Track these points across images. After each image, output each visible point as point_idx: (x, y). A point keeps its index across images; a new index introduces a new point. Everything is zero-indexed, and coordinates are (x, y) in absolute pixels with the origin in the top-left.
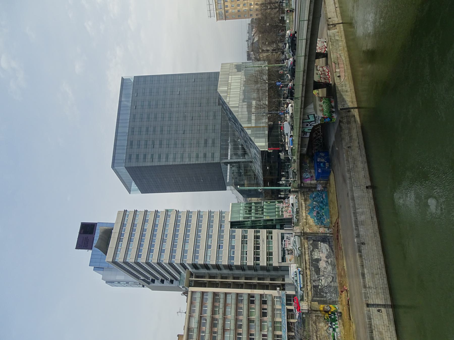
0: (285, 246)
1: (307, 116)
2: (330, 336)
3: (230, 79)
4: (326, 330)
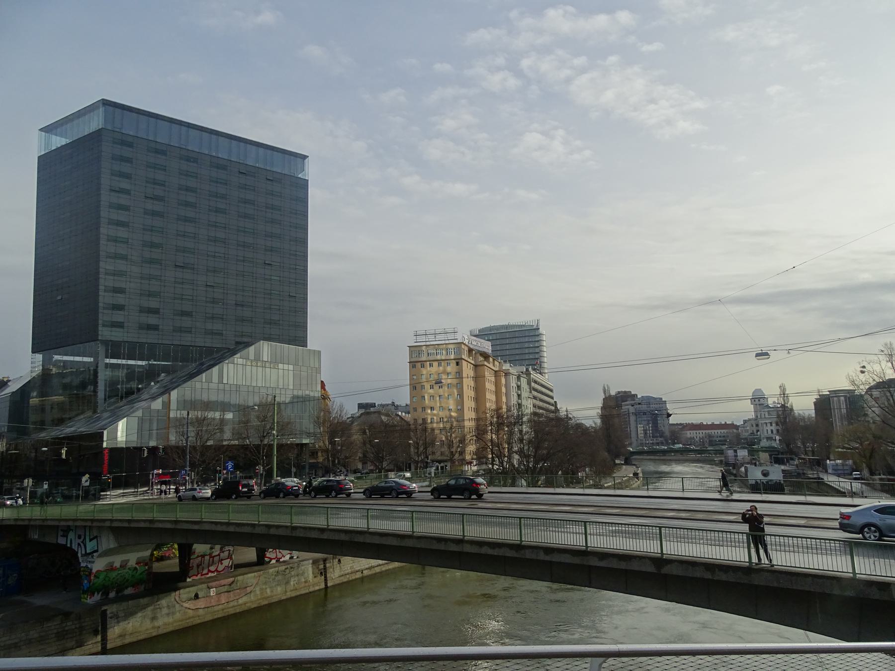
1: (95, 535)
3: (286, 367)
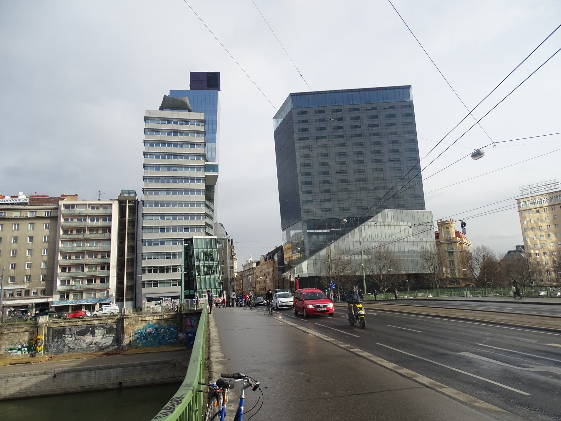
0: (165, 300)
2: (14, 345)
4: (19, 342)
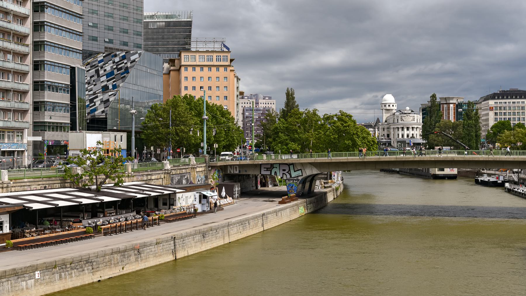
1: (299, 169)
